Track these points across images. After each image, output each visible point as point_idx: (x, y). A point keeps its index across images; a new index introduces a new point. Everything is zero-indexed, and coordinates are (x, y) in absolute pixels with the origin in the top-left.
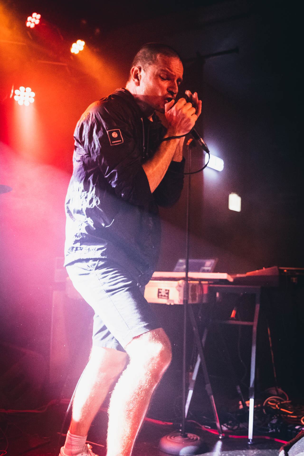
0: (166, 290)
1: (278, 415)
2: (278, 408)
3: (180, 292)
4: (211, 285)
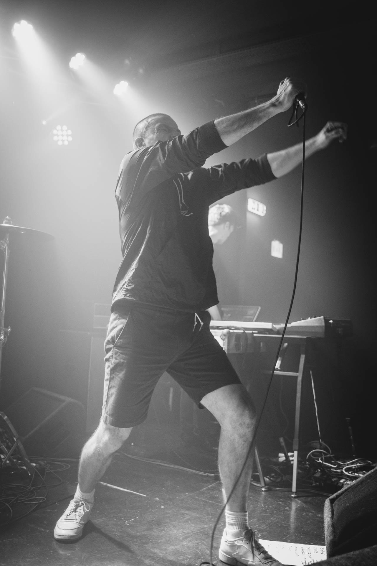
1: (322, 469)
2: (322, 462)
3: (224, 341)
4: (255, 335)
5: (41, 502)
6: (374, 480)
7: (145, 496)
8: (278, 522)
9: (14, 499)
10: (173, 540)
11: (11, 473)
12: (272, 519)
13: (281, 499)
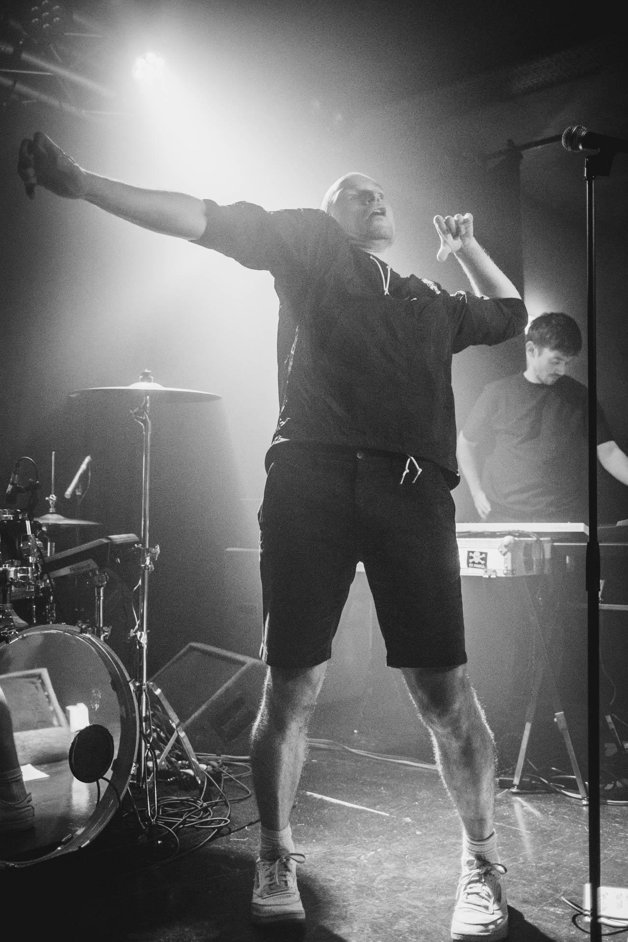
0: (481, 553)
3: (506, 557)
4: (556, 544)
5: (220, 825)
7: (388, 815)
8: (616, 857)
9: (179, 820)
10: (442, 887)
11: (169, 780)
12: (606, 852)
13: (618, 819)
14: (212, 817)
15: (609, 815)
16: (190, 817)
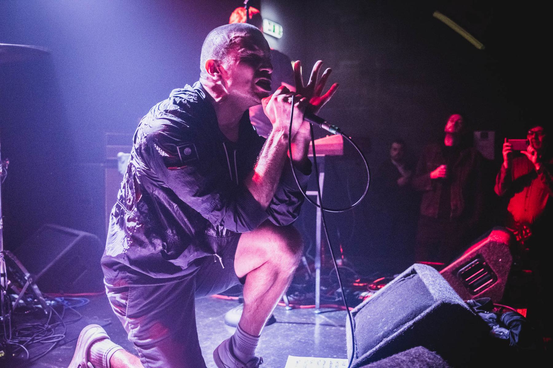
5: (60, 339)
6: (394, 291)
9: (29, 339)
14: (54, 335)
15: (300, 314)
16: (38, 336)
